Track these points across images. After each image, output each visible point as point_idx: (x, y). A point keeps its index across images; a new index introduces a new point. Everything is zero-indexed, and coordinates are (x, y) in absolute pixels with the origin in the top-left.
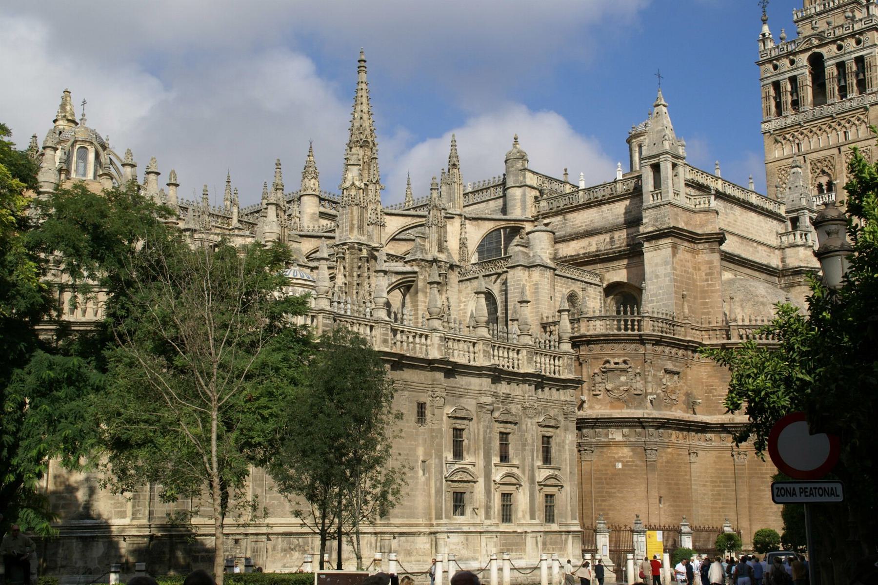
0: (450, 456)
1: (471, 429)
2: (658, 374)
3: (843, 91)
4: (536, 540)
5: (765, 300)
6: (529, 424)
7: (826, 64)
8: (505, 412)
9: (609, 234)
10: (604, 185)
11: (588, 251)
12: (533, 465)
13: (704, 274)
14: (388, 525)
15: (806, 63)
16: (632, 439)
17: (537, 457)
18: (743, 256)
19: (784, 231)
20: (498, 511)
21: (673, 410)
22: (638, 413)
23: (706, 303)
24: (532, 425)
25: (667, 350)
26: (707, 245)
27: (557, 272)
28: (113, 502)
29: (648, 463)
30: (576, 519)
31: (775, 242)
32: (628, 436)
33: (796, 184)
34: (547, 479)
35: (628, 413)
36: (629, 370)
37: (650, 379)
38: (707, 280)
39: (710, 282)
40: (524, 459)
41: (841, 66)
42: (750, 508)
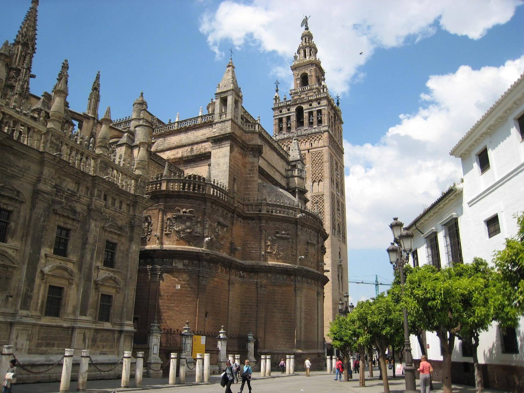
1: (22, 214)
2: (213, 224)
3: (311, 124)
4: (84, 335)
6: (93, 225)
7: (304, 112)
8: (68, 207)
9: (190, 147)
10: (191, 119)
11: (176, 156)
13: (248, 170)
15: (295, 111)
16: (190, 268)
17: (98, 258)
20: (43, 302)
23: (248, 188)
25: (221, 210)
26: (251, 153)
29: (200, 287)
30: (131, 320)
32: (188, 265)
33: (295, 148)
34: (105, 279)
36: (193, 218)
37: (207, 226)
38: (250, 174)
39: (251, 175)
40: (82, 257)
41: (311, 113)
42: (265, 323)
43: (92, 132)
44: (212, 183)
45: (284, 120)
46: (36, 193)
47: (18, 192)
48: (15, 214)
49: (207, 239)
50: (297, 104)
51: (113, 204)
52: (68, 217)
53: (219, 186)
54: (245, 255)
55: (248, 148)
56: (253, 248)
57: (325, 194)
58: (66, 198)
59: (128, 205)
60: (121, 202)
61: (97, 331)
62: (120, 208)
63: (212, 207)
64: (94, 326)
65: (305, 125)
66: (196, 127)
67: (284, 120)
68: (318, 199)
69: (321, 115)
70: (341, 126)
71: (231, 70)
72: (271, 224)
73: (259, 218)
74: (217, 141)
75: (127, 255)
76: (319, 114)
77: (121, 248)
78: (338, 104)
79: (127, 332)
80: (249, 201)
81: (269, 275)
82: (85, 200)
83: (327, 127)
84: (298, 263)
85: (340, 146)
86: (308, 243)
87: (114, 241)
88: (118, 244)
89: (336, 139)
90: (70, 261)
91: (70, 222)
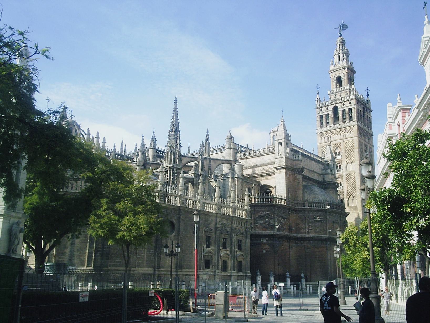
0: (205, 246)
1: (213, 237)
2: (279, 218)
3: (344, 119)
5: (317, 193)
6: (233, 235)
7: (339, 110)
12: (235, 250)
13: (296, 183)
14: (182, 271)
16: (269, 242)
18: (310, 177)
19: (324, 168)
21: (284, 231)
22: (272, 233)
24: (234, 235)
27: (244, 180)
28: (80, 260)
30: (249, 271)
31: (321, 172)
34: (239, 256)
35: (268, 232)
38: (297, 185)
40: (231, 248)
41: (344, 111)
43: (209, 167)
44: (277, 197)
45: (324, 117)
46: (216, 228)
47: (211, 229)
48: (211, 237)
49: (277, 227)
50: (334, 104)
51: (239, 224)
52: (226, 234)
53: (281, 197)
54: (297, 231)
55: (296, 170)
56: (302, 227)
57: (356, 172)
58: (224, 227)
59: (244, 223)
60: (241, 223)
61: (238, 276)
62: (241, 225)
63: (278, 210)
64: (237, 274)
65: (339, 121)
66: (264, 155)
67: (324, 117)
68: (351, 176)
69: (352, 112)
70: (370, 115)
71: (283, 124)
72: (311, 214)
73: (304, 210)
74: (278, 169)
75: (246, 244)
76: (350, 111)
77: (243, 241)
78: (368, 95)
79: (248, 276)
80: (298, 201)
81: (311, 242)
82: (230, 226)
83: (356, 122)
84: (328, 234)
85: (370, 132)
86: (334, 222)
87: (241, 239)
88: (243, 240)
89: (365, 128)
90: (228, 250)
91: (226, 235)
